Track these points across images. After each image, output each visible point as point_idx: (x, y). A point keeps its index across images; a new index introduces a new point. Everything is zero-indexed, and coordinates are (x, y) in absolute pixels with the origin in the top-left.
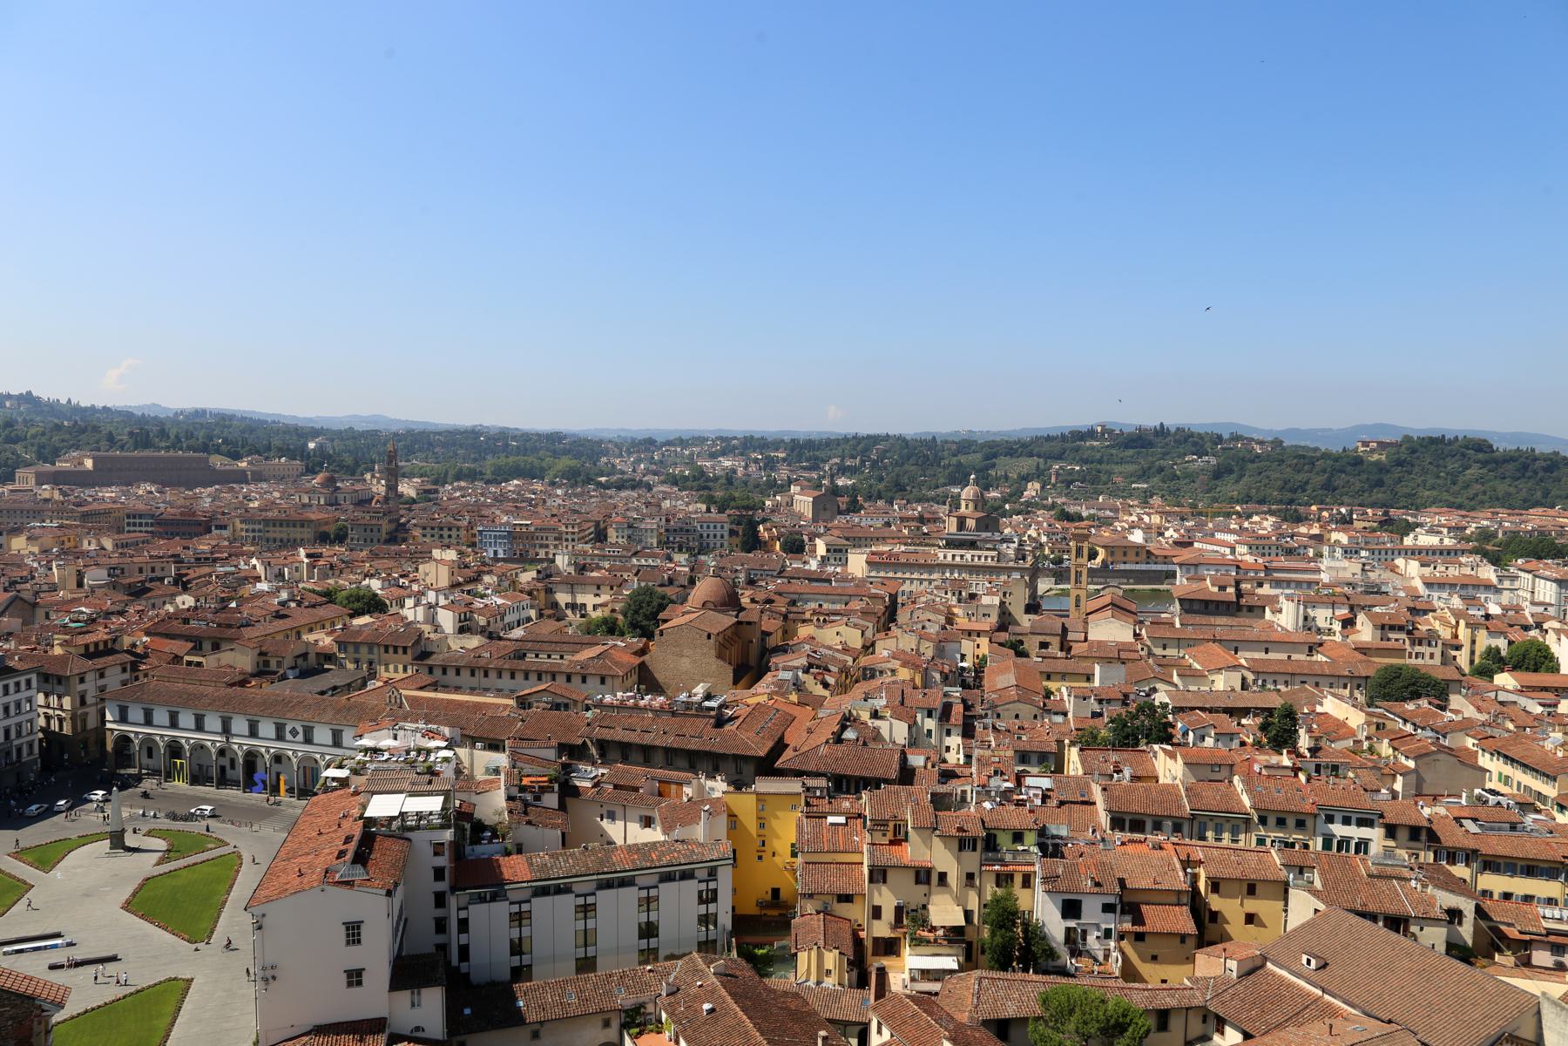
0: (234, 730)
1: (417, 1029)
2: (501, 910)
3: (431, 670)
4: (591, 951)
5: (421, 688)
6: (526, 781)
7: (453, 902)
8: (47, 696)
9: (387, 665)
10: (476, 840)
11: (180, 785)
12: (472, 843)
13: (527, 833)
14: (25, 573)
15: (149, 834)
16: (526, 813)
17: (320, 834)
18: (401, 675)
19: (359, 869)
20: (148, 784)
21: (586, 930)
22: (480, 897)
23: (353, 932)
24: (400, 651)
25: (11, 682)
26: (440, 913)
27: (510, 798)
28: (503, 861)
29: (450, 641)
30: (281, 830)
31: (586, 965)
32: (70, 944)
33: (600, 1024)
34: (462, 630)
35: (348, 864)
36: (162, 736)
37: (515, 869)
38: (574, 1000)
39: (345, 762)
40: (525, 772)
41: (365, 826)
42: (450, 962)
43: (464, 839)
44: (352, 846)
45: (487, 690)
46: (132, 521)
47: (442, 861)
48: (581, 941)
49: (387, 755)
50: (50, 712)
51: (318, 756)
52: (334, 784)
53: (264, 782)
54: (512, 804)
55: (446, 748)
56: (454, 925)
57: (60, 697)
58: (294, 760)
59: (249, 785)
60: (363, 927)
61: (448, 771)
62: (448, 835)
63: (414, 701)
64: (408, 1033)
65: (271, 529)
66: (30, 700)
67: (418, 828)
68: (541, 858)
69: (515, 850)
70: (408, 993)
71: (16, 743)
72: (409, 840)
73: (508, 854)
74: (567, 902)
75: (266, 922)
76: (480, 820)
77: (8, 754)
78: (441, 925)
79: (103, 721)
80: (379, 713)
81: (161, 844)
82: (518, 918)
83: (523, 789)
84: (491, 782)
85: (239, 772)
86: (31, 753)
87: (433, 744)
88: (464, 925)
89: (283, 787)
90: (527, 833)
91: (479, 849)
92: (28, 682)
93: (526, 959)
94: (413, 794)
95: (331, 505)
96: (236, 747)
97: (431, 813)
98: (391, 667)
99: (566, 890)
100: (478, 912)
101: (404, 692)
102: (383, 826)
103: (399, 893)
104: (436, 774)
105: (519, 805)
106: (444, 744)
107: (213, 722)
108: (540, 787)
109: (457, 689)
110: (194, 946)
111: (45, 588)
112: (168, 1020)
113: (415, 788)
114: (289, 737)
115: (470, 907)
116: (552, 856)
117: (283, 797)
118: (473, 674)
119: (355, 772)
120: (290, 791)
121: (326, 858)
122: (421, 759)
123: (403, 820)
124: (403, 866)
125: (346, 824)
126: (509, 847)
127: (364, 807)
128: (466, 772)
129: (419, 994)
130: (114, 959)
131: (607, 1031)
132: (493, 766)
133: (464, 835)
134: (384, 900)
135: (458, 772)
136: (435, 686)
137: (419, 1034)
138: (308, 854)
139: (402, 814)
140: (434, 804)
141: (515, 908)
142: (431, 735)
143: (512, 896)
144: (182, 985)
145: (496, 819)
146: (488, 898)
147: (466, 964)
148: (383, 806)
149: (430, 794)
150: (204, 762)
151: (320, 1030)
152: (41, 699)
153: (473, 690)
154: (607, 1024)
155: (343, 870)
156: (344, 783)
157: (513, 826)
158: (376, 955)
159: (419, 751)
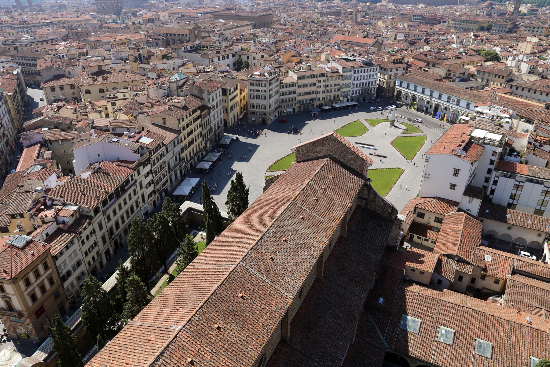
0: (434, 96)
1: (468, 210)
2: (511, 182)
3: (511, 87)
4: (543, 208)
5: (505, 93)
6: (538, 138)
7: (494, 173)
8: (381, 74)
9: (494, 82)
10: (510, 154)
11: (413, 110)
12: (508, 155)
13: (531, 157)
14: (380, 33)
15: (401, 123)
16: (534, 150)
17: (454, 137)
18: (499, 87)
19: (464, 152)
20: (404, 108)
21: (544, 200)
22: (505, 175)
23: (456, 172)
24: (501, 77)
25: (372, 68)
26: (488, 176)
27: (529, 143)
28: (519, 165)
29: (523, 77)
30: (441, 132)
31: (539, 212)
32: (375, 149)
33: (537, 234)
34: (530, 73)
35: (461, 150)
36: (411, 93)
37: (522, 169)
38: (529, 222)
39: (469, 115)
40: (539, 134)
41: (470, 139)
42: (486, 193)
43: (505, 153)
44: (464, 145)
45: (533, 99)
46: (415, 17)
47: (495, 158)
48: (540, 203)
49: (485, 116)
50: (381, 79)
51: (460, 111)
52: (463, 121)
53: (439, 115)
54: (529, 145)
55: (509, 118)
56: (492, 182)
57: (384, 75)
58: (451, 110)
59: (435, 115)
60: (460, 171)
61: (507, 127)
62: (500, 150)
63: (501, 98)
64: (465, 210)
65: (462, 24)
66: (376, 75)
67: (489, 144)
68: (535, 168)
69: (524, 162)
70: (469, 197)
71: (371, 87)
72: (484, 147)
73: (521, 163)
74: (540, 188)
75: (430, 160)
76: (514, 148)
77: (368, 90)
78: (487, 180)
79: (395, 85)
80: (486, 99)
81: (404, 127)
82: (517, 187)
83: (536, 141)
84: (523, 135)
85: (432, 111)
86: (374, 91)
87: (504, 115)
88: (495, 182)
89: (445, 119)
90: (531, 157)
91: (510, 158)
92: (377, 69)
93: (515, 202)
94: (491, 132)
95: (488, 15)
96: (433, 101)
97: (495, 140)
98: (496, 83)
99: (542, 183)
100: (502, 180)
101: (498, 94)
102: (476, 140)
103: (476, 165)
104: (502, 127)
105: (532, 146)
106: (508, 116)
107: (428, 92)
108: (544, 142)
109: (521, 96)
110: (407, 161)
111: (385, 39)
112: (396, 179)
113: (492, 130)
114: (451, 102)
115: (500, 177)
116: (539, 169)
117: (445, 122)
118: (529, 91)
119: (472, 119)
120: (447, 120)
121: (454, 146)
122: (497, 120)
123: (484, 140)
124: (479, 156)
125: (464, 136)
126: (523, 161)
127: (472, 132)
128: (514, 129)
129: (472, 199)
130: (385, 157)
131: (538, 238)
132: (526, 129)
133: (506, 151)
134: (470, 165)
135: (511, 128)
136: (511, 93)
137: (469, 212)
138: (448, 143)
139: (485, 138)
140: (498, 137)
141: (517, 183)
142: (504, 112)
143: (517, 178)
144: (402, 171)
145: (521, 149)
146: (508, 176)
147: (492, 196)
148: (478, 133)
149: (497, 133)
150: (422, 105)
151: (438, 198)
152: (379, 75)
153: (527, 98)
154: (539, 235)
155: (459, 151)
156: (466, 122)
157: (527, 153)
158: (462, 182)
159: (498, 117)
